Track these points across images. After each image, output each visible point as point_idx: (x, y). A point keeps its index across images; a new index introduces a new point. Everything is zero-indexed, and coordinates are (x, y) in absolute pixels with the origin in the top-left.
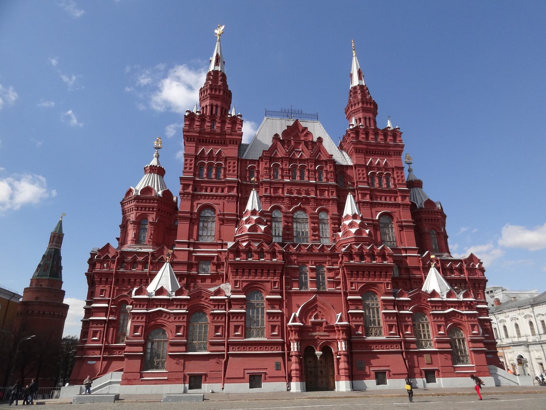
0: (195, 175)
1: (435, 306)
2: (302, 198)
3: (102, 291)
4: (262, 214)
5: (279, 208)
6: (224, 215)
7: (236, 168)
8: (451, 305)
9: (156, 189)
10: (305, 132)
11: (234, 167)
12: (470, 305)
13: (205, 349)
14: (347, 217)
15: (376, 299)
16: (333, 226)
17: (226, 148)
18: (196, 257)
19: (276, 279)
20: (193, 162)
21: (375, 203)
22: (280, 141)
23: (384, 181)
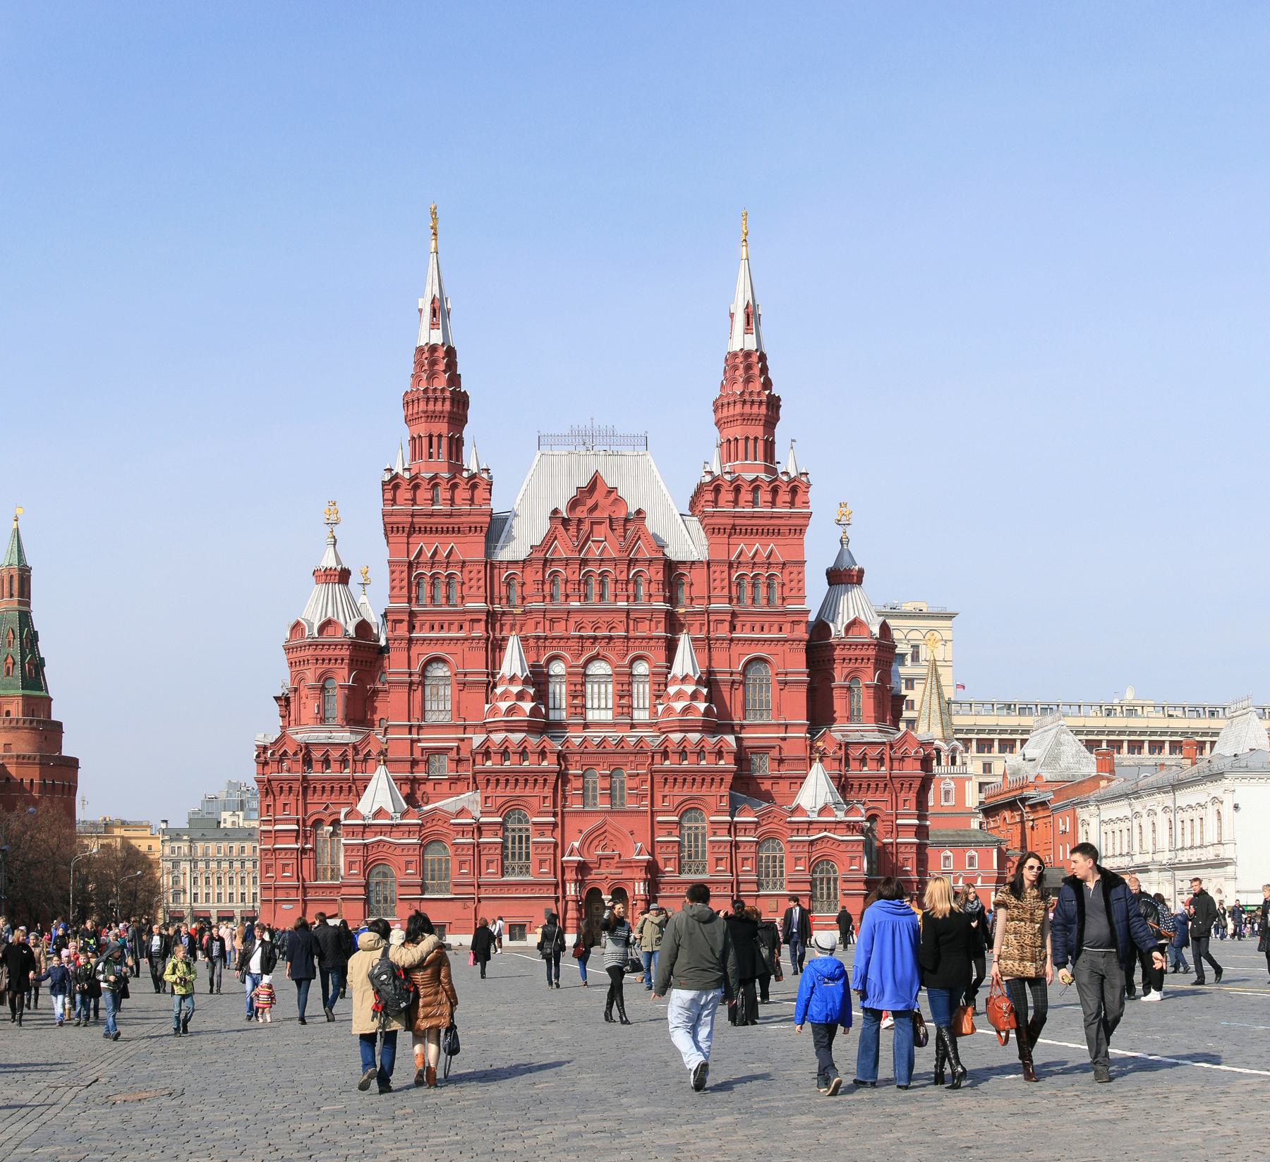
0: (409, 601)
3: (285, 805)
6: (465, 674)
7: (482, 582)
8: (823, 826)
9: (342, 620)
12: (851, 827)
13: (447, 891)
15: (703, 821)
18: (423, 749)
19: (548, 791)
20: (405, 575)
21: (739, 640)
22: (565, 522)
23: (762, 592)
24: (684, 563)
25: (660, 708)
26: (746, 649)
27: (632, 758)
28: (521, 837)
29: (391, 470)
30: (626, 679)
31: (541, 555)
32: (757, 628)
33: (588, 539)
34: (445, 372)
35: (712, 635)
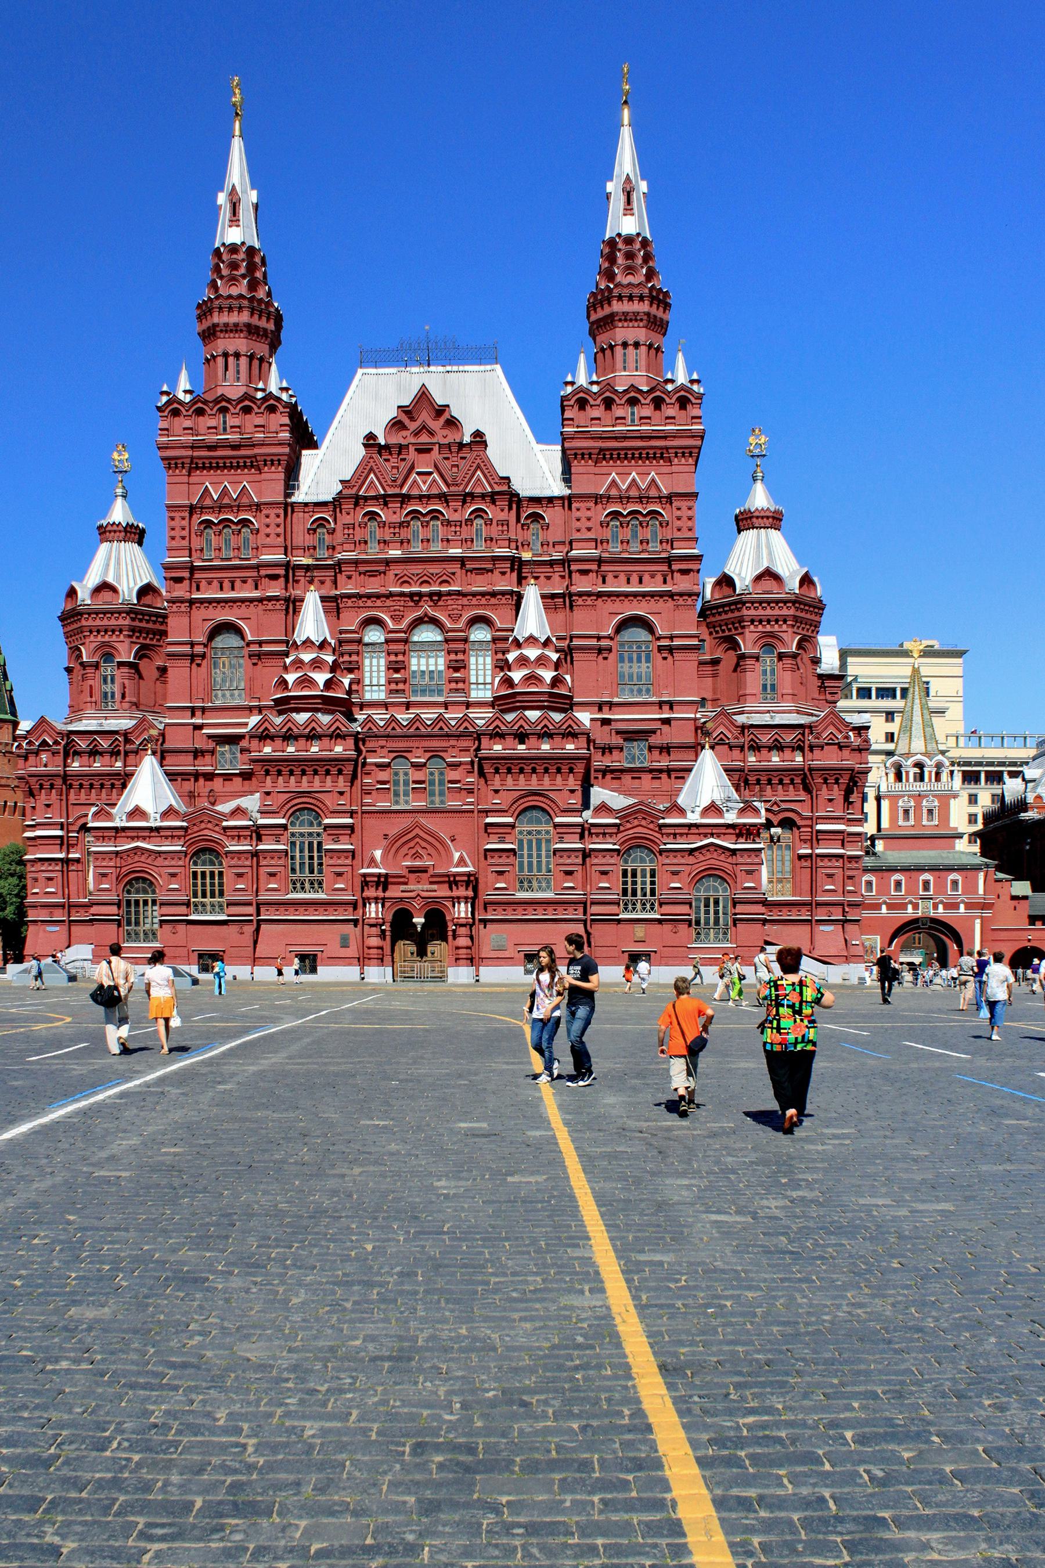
1: (675, 835)
2: (431, 595)
4: (323, 645)
5: (378, 622)
7: (281, 530)
10: (442, 420)
11: (278, 526)
14: (518, 644)
16: (500, 656)
17: (258, 478)
20: (185, 523)
21: (609, 595)
22: (382, 449)
24: (536, 500)
25: (497, 680)
26: (616, 606)
27: (453, 742)
28: (311, 844)
29: (167, 393)
30: (460, 646)
31: (353, 491)
32: (635, 578)
33: (412, 468)
34: (244, 276)
35: (574, 589)
